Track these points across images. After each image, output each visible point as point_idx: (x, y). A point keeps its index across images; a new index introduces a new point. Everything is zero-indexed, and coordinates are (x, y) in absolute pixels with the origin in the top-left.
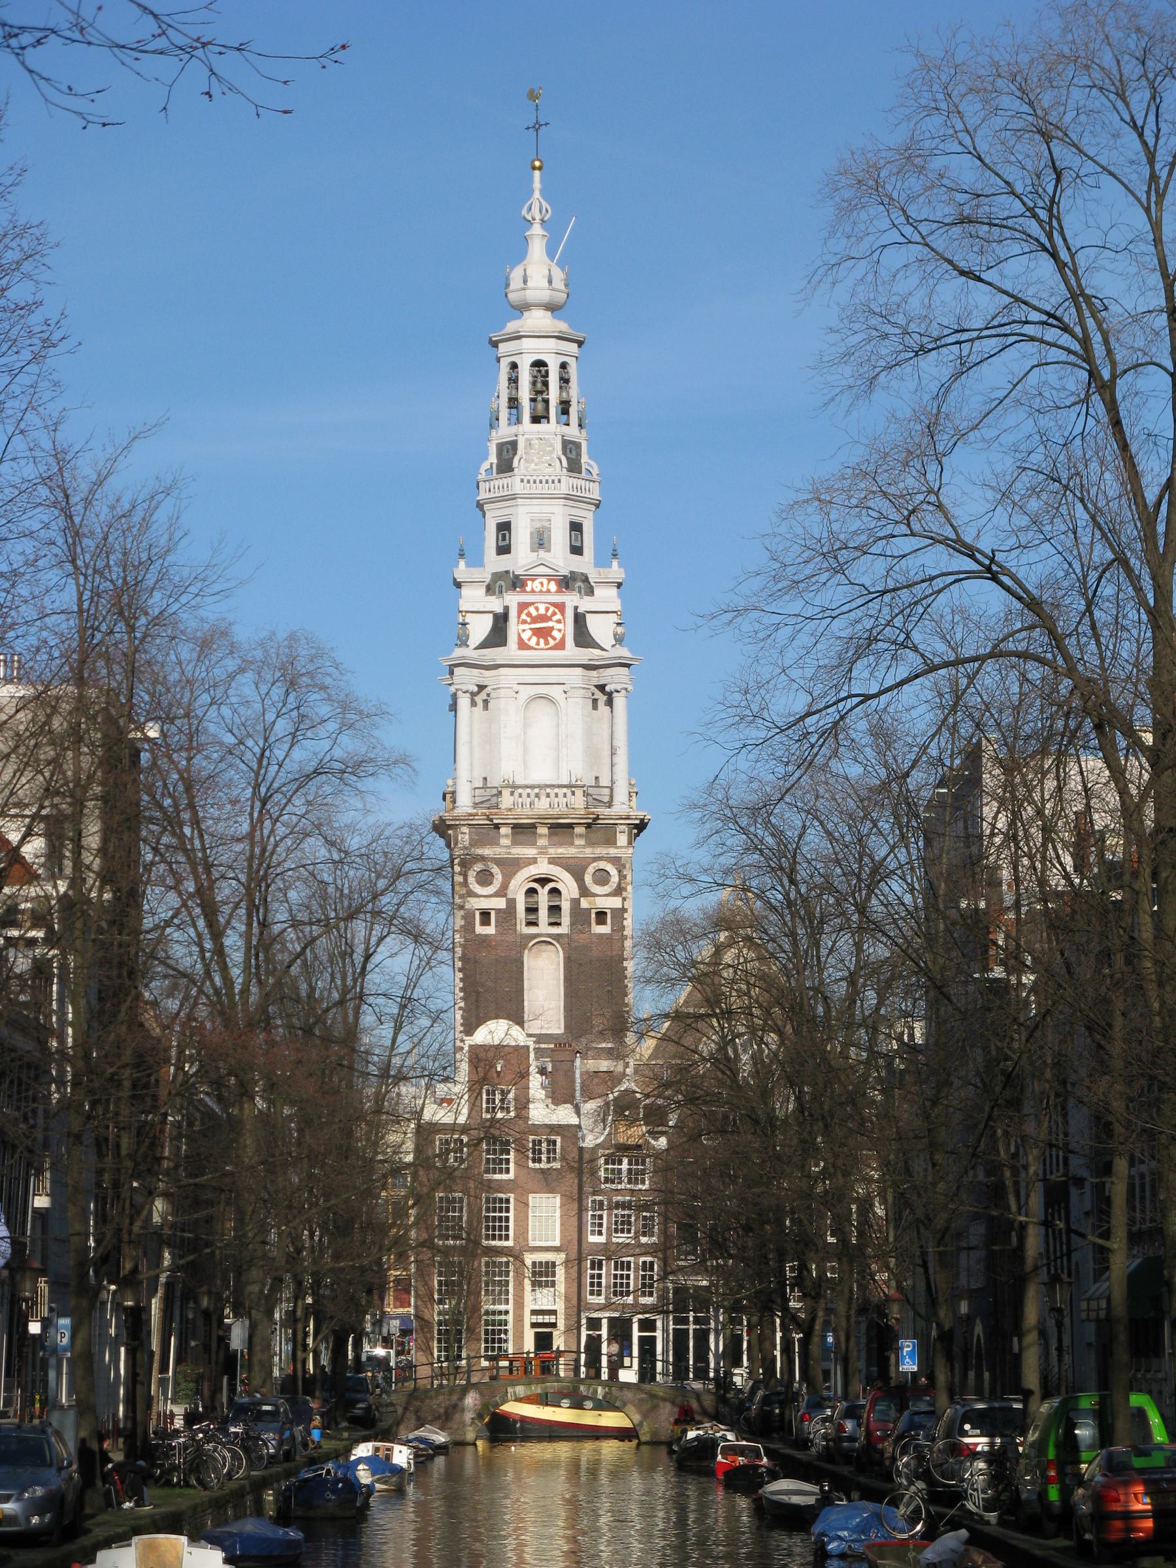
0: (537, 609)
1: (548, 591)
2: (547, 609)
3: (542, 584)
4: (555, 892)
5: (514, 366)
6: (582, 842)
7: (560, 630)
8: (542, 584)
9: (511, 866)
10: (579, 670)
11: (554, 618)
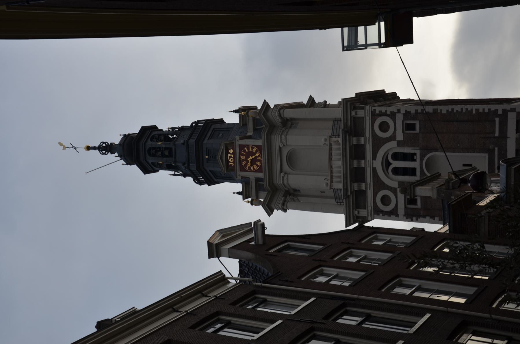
0: (243, 160)
1: (233, 153)
2: (243, 155)
3: (230, 157)
4: (396, 156)
5: (153, 163)
6: (362, 139)
7: (252, 149)
8: (230, 157)
9: (379, 185)
10: (273, 137)
11: (247, 151)
